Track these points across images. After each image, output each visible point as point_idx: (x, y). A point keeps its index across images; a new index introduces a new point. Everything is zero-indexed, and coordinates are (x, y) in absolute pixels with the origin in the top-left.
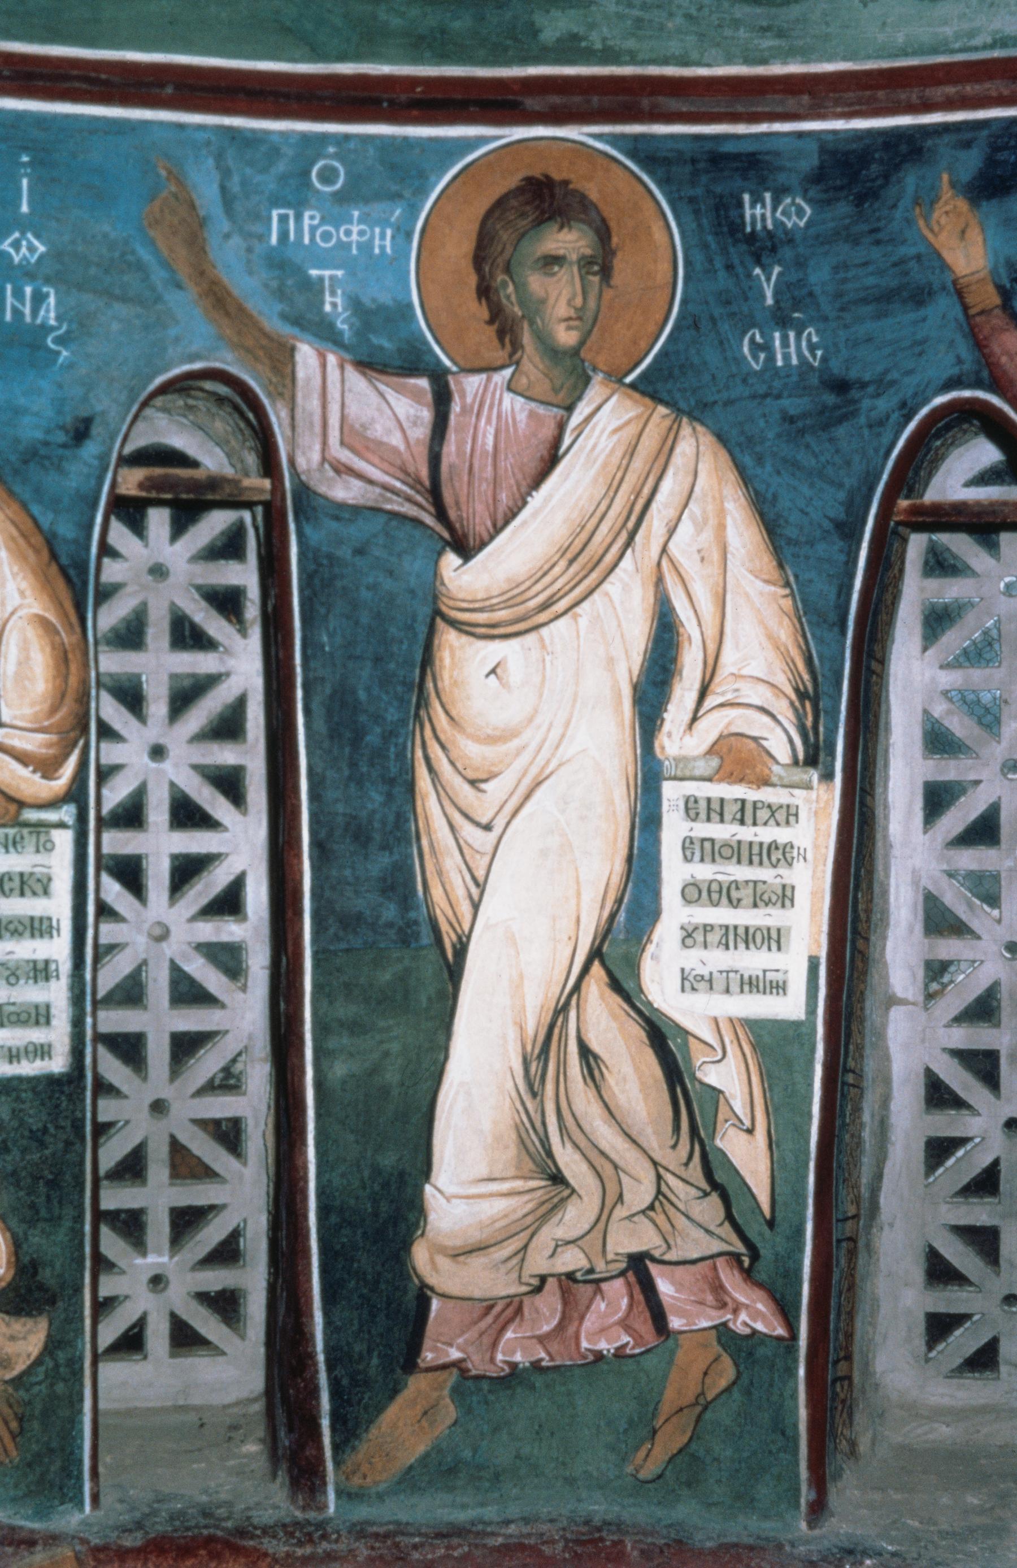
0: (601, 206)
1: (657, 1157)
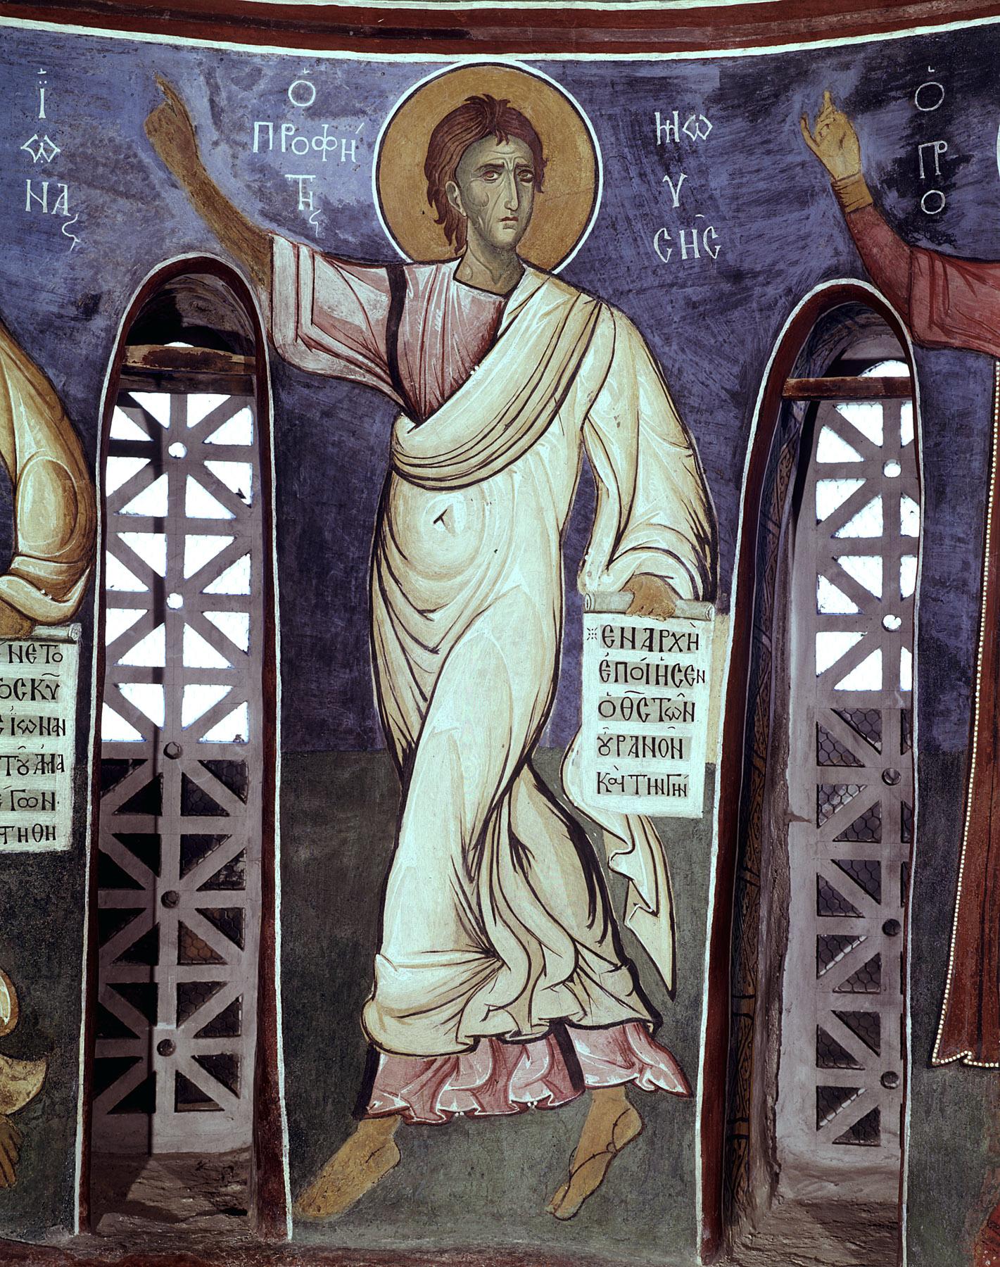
0: (534, 122)
1: (576, 936)
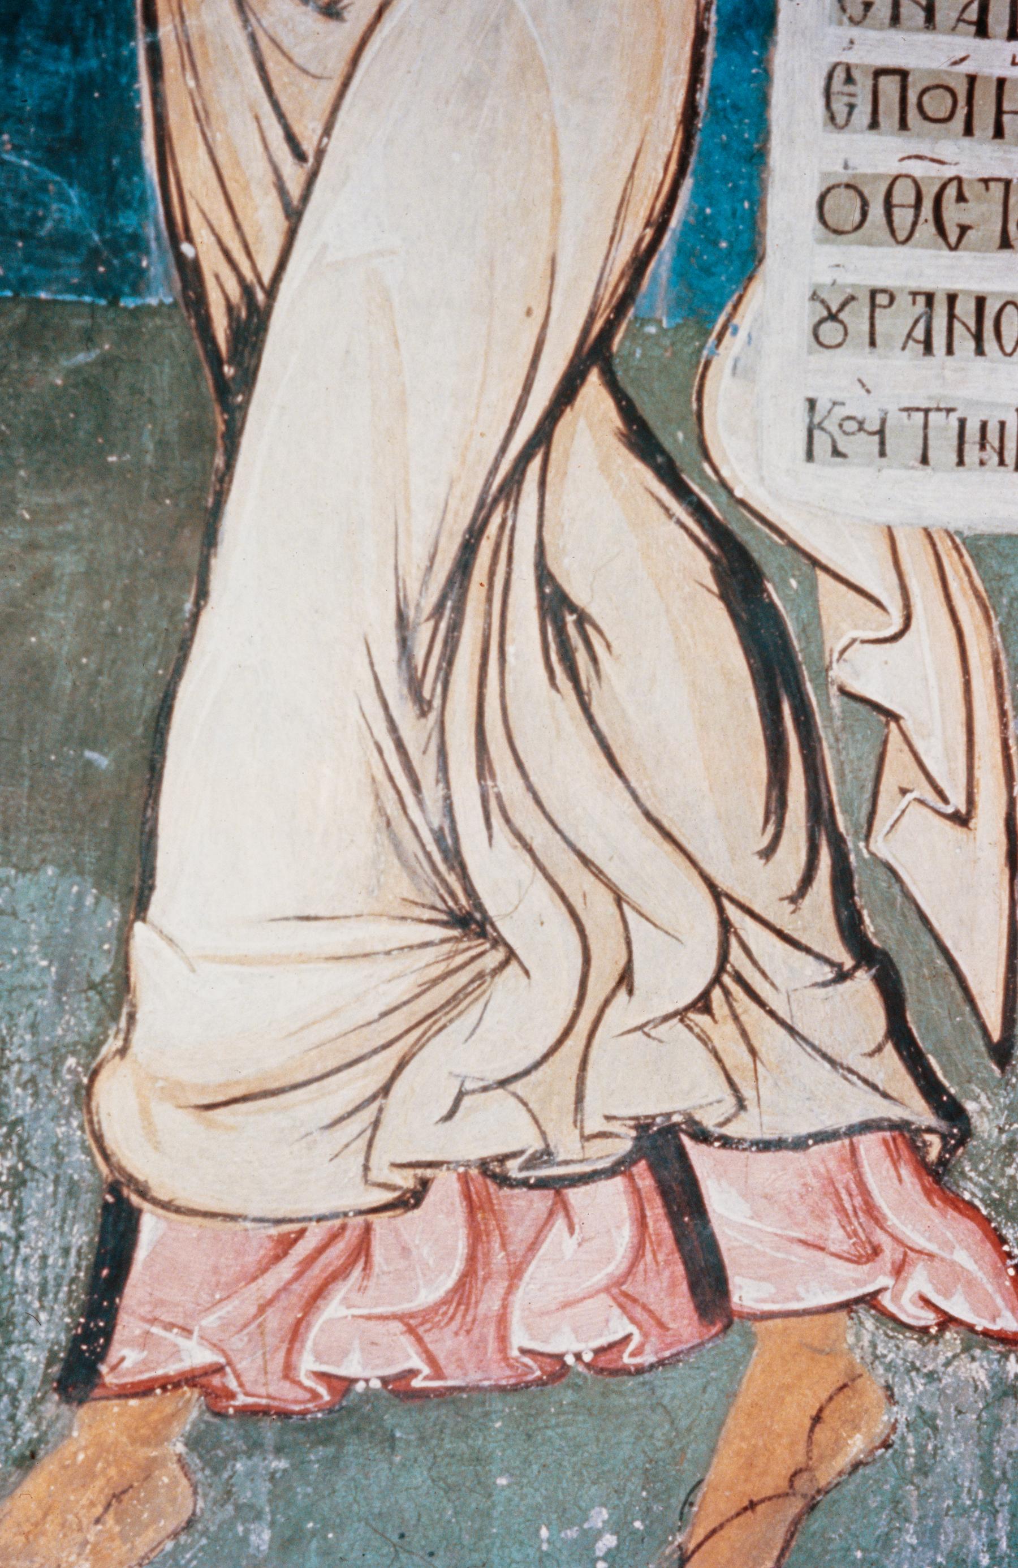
1: (723, 883)
